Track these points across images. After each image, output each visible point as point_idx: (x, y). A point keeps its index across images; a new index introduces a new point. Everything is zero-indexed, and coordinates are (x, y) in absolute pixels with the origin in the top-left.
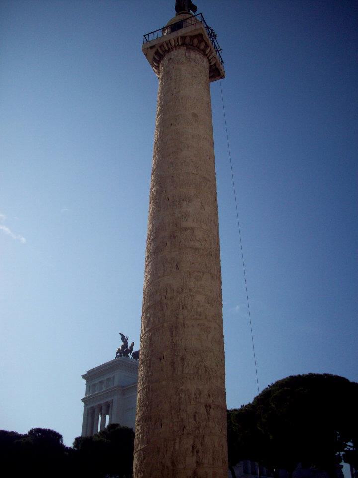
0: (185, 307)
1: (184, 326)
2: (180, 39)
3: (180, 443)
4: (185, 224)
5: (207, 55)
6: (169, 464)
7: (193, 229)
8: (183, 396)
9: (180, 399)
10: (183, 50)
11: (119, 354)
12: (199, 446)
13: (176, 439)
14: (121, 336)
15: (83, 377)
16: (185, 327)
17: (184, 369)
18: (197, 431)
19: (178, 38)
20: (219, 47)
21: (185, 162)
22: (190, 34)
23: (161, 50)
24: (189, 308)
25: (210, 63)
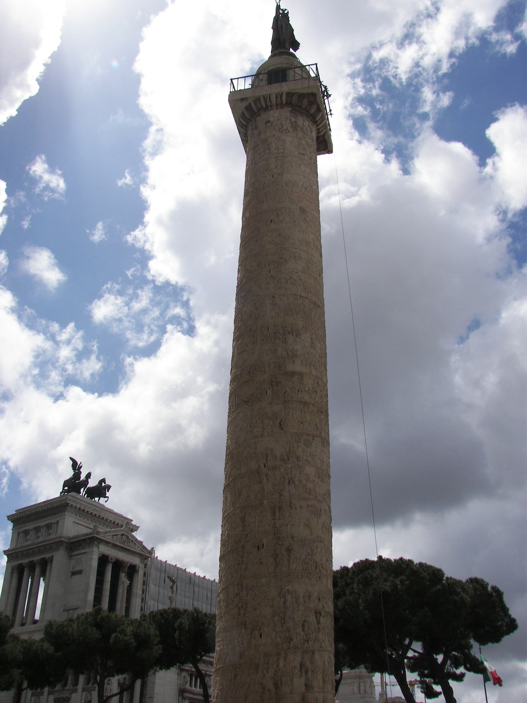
0: (291, 482)
1: (291, 506)
2: (284, 94)
3: (285, 659)
4: (290, 367)
5: (317, 122)
6: (272, 687)
7: (301, 375)
8: (289, 598)
9: (285, 603)
10: (286, 112)
11: (66, 488)
12: (308, 664)
13: (279, 654)
14: (71, 462)
15: (11, 518)
16: (291, 507)
17: (291, 564)
18: (306, 644)
19: (282, 94)
20: (330, 110)
21: (291, 278)
22: (300, 91)
23: (256, 105)
24: (297, 483)
25: (319, 133)
